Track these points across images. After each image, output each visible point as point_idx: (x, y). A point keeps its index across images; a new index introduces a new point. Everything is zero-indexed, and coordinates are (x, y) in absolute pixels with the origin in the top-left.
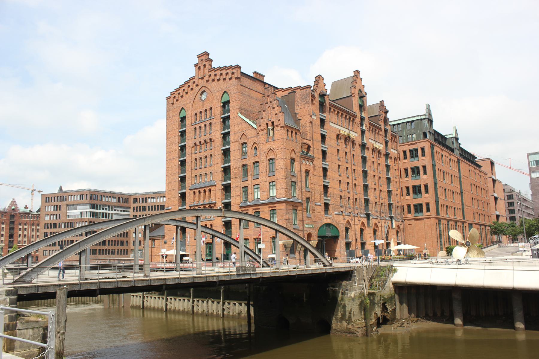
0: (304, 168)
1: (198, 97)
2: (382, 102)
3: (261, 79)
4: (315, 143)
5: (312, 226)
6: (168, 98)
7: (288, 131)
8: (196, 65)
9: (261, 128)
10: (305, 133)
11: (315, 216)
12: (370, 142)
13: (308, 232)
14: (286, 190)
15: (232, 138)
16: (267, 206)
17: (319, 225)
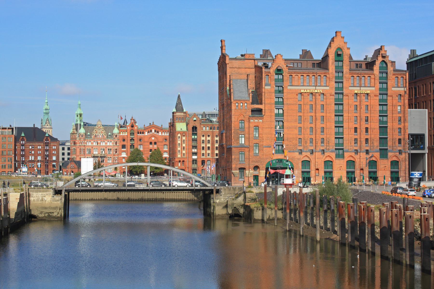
11: (263, 155)
12: (351, 90)
13: (255, 165)
17: (268, 160)
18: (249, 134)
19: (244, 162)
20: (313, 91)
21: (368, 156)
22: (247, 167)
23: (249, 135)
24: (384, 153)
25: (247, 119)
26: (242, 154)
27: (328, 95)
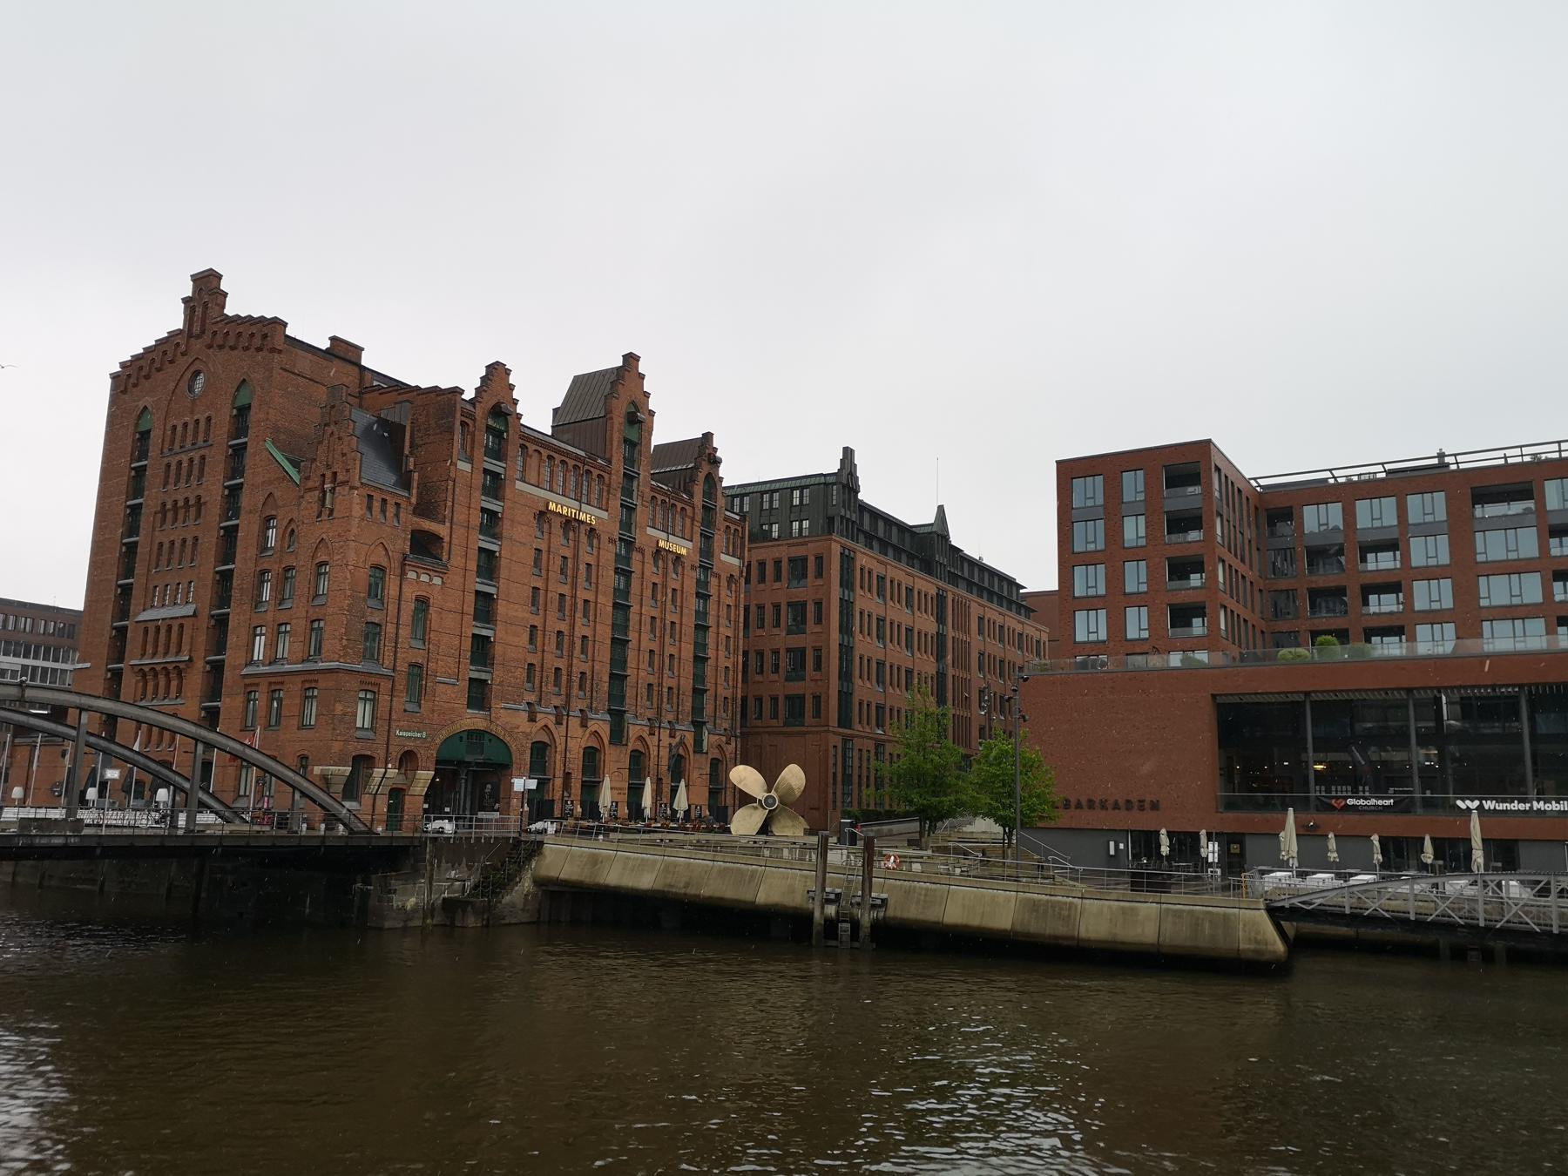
0: (410, 593)
1: (184, 385)
2: (708, 437)
3: (349, 356)
4: (459, 532)
5: (419, 735)
6: (115, 377)
7: (370, 497)
8: (186, 301)
9: (310, 484)
10: (435, 505)
14: (345, 642)
15: (245, 500)
16: (299, 679)
17: (444, 734)
18: (398, 624)
19: (370, 735)
20: (575, 513)
21: (675, 742)
22: (380, 753)
23: (397, 629)
24: (618, 735)
25: (397, 564)
26: (365, 700)
27: (604, 538)
